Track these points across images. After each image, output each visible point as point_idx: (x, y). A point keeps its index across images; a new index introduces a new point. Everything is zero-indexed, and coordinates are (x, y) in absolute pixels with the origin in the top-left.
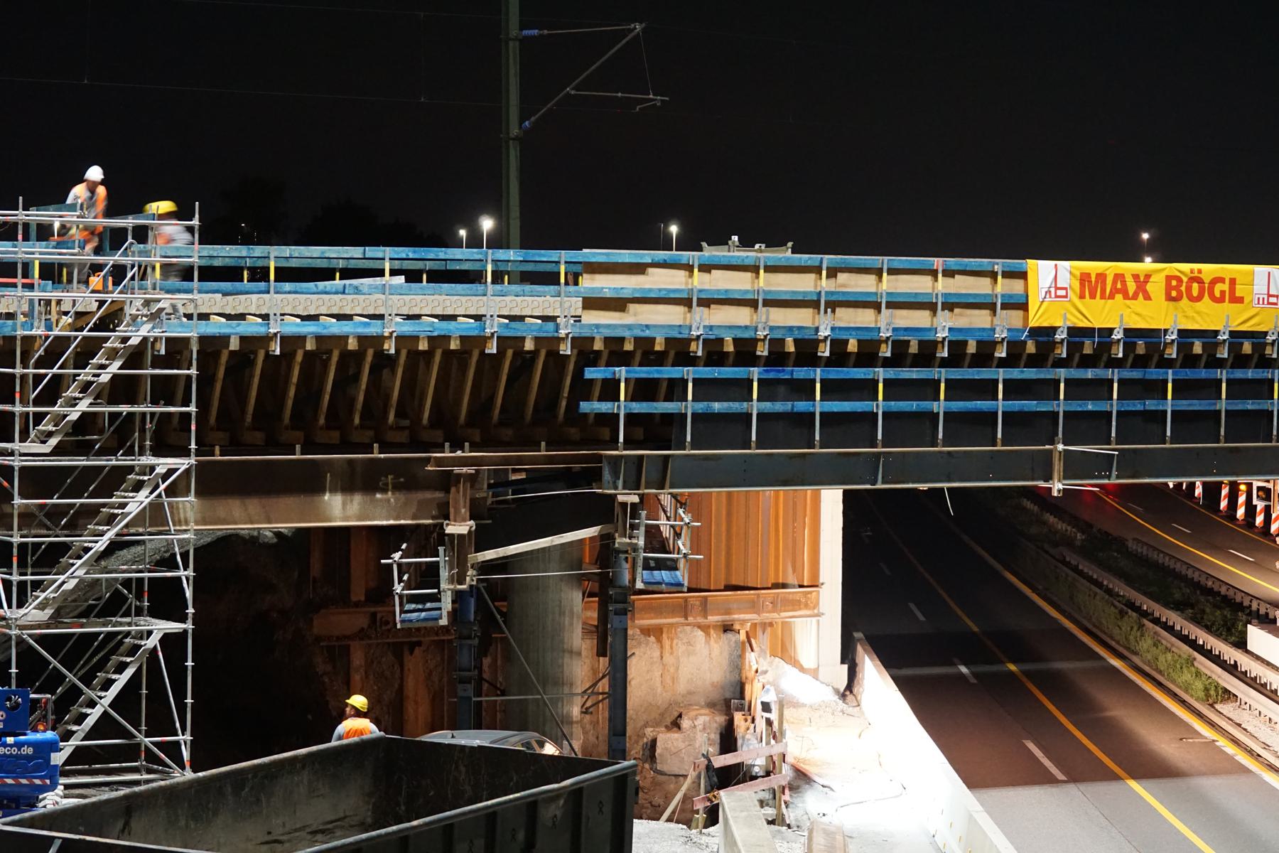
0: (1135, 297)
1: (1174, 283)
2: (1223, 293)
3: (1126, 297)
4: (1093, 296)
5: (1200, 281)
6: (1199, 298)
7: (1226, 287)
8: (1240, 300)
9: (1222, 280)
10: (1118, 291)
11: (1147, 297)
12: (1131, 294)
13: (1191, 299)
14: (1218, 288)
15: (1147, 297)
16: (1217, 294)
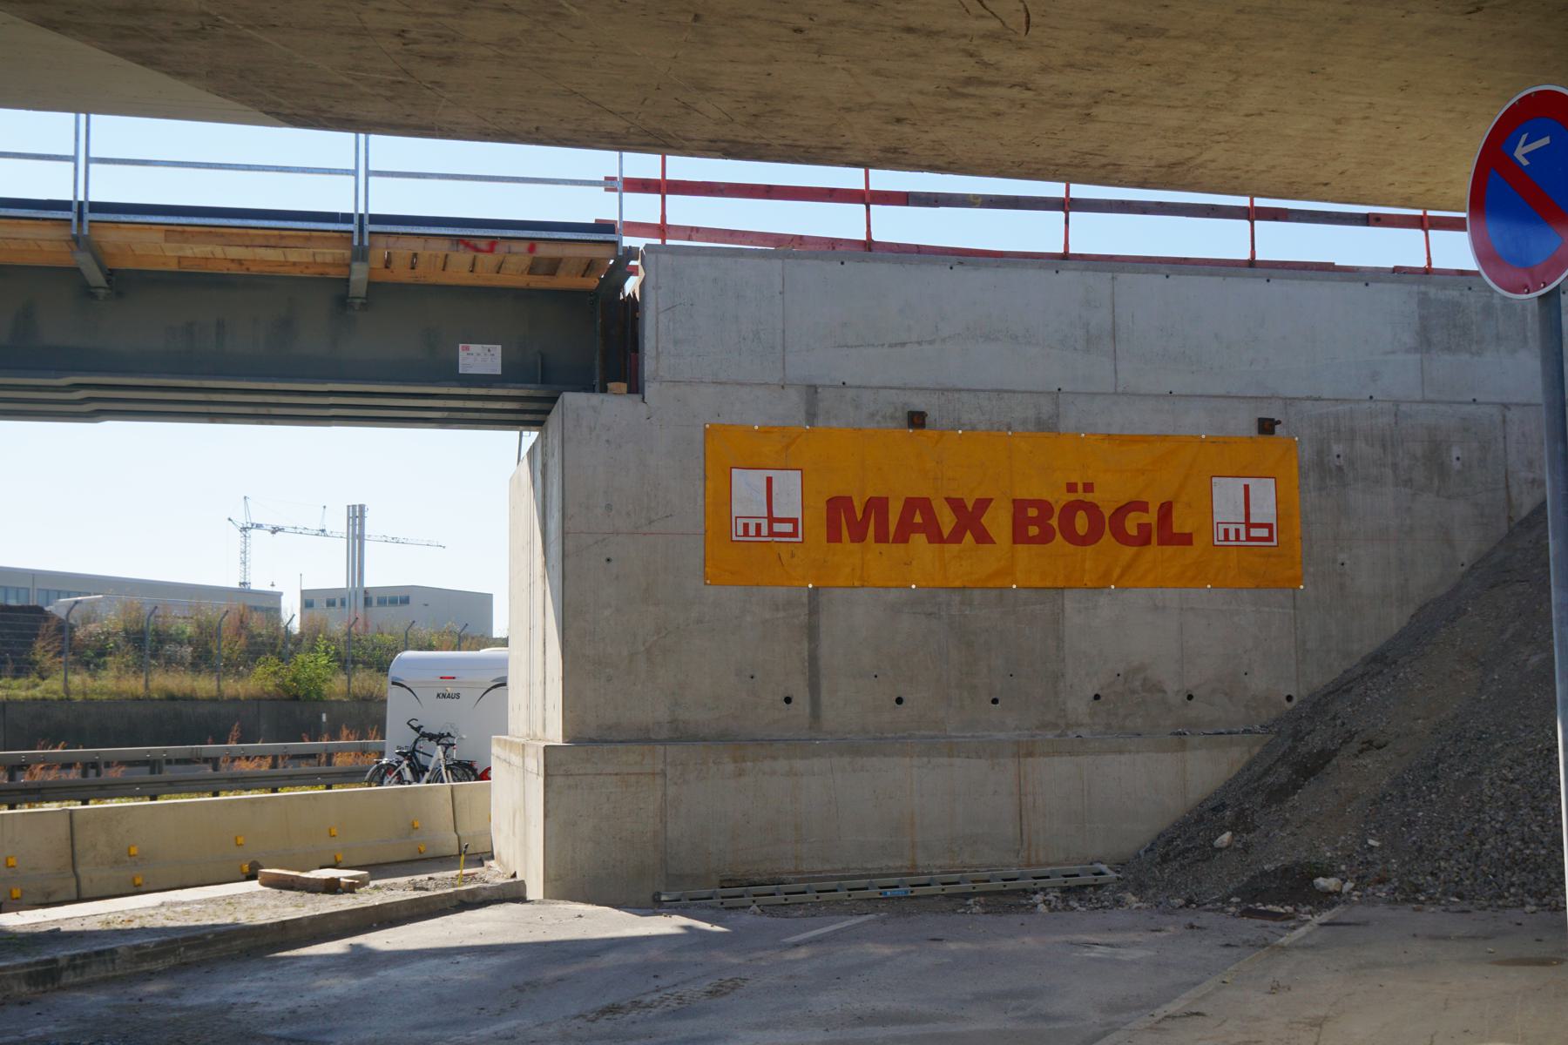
0: (956, 537)
1: (1033, 512)
2: (1144, 529)
3: (936, 537)
4: (858, 536)
5: (1092, 509)
6: (1092, 537)
7: (1151, 518)
8: (1186, 540)
9: (1142, 507)
10: (918, 529)
12: (946, 532)
13: (1072, 537)
14: (1131, 525)
15: (983, 537)
16: (1131, 528)
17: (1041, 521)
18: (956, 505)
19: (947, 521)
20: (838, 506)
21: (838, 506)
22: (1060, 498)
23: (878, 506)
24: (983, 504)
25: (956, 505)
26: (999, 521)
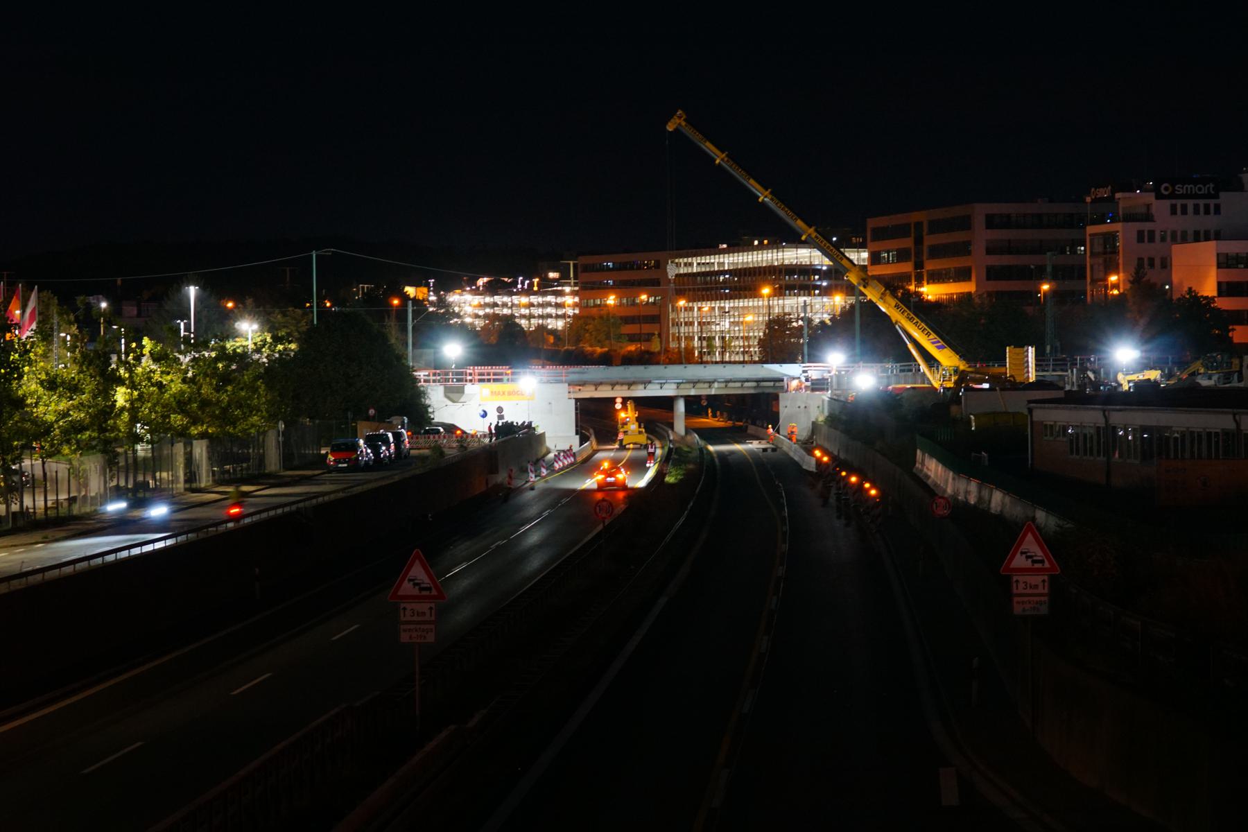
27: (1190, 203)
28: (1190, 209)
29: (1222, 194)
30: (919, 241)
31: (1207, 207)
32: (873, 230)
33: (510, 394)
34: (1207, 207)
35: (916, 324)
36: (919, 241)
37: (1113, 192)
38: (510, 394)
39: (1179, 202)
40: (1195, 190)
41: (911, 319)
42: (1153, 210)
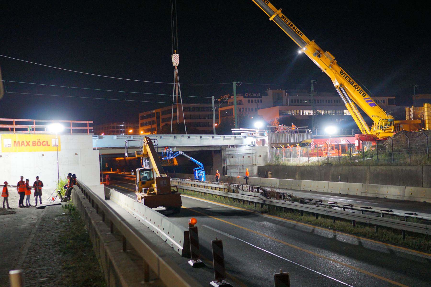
0: (27, 146)
3: (25, 146)
5: (40, 142)
6: (40, 145)
7: (46, 143)
8: (49, 145)
9: (45, 142)
11: (29, 146)
14: (44, 143)
15: (29, 146)
17: (35, 144)
18: (27, 142)
19: (26, 144)
20: (15, 142)
21: (15, 142)
22: (37, 141)
23: (19, 142)
24: (29, 142)
25: (27, 142)
26: (31, 144)
27: (254, 99)
28: (254, 101)
29: (263, 97)
30: (158, 118)
31: (258, 101)
32: (141, 117)
33: (34, 144)
34: (258, 101)
35: (355, 86)
36: (158, 118)
37: (230, 96)
38: (34, 144)
39: (250, 99)
40: (255, 95)
41: (352, 83)
42: (243, 101)
